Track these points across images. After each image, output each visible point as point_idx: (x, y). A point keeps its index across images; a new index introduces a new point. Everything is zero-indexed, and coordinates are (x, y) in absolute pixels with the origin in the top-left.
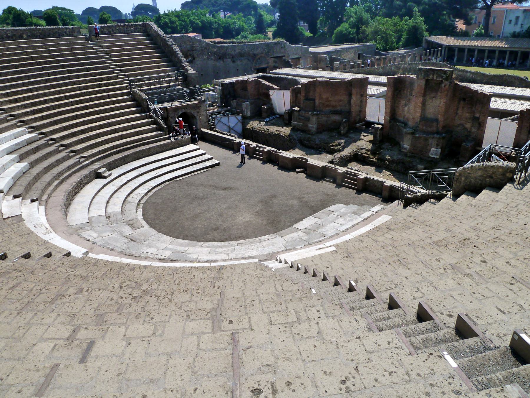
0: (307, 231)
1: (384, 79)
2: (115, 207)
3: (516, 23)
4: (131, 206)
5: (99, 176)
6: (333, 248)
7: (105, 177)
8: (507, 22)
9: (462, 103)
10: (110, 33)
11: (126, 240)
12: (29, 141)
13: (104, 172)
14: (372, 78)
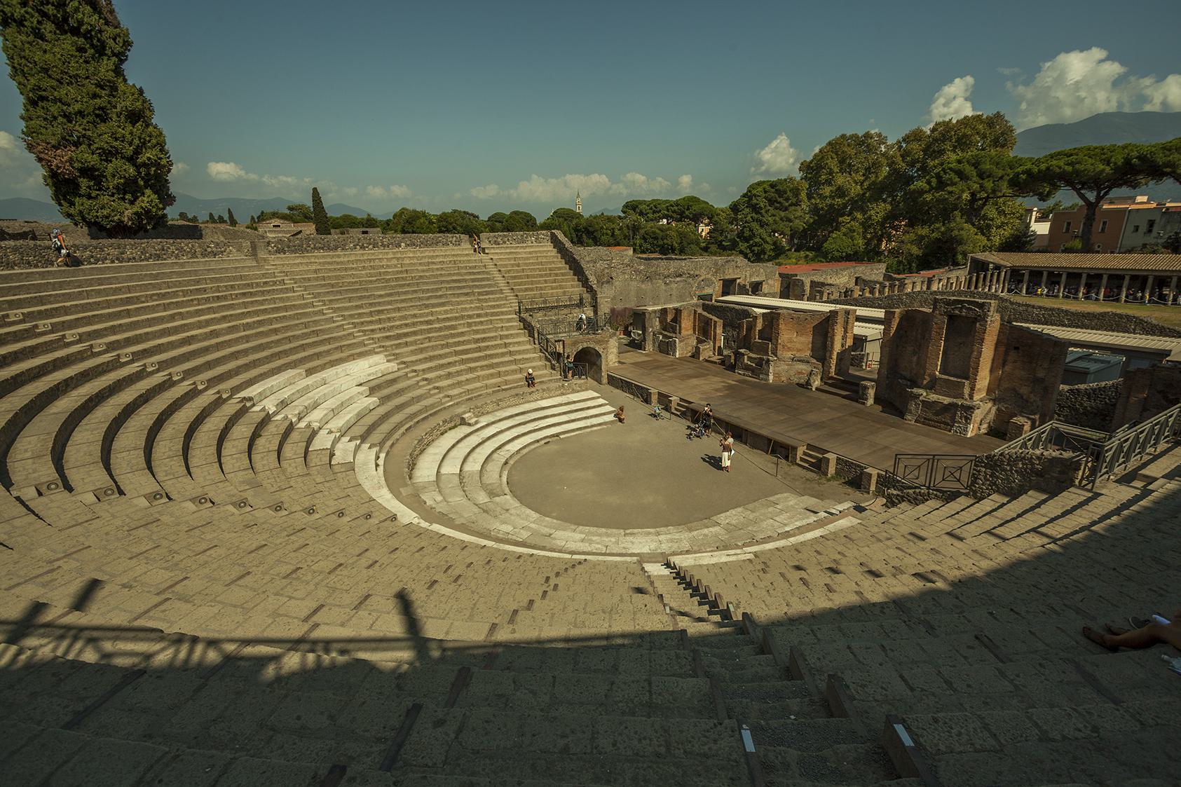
0: (730, 529)
1: (880, 313)
2: (474, 466)
3: (1150, 231)
4: (494, 468)
5: (463, 422)
6: (751, 556)
7: (469, 425)
8: (1131, 228)
9: (1013, 354)
11: (476, 510)
14: (862, 311)
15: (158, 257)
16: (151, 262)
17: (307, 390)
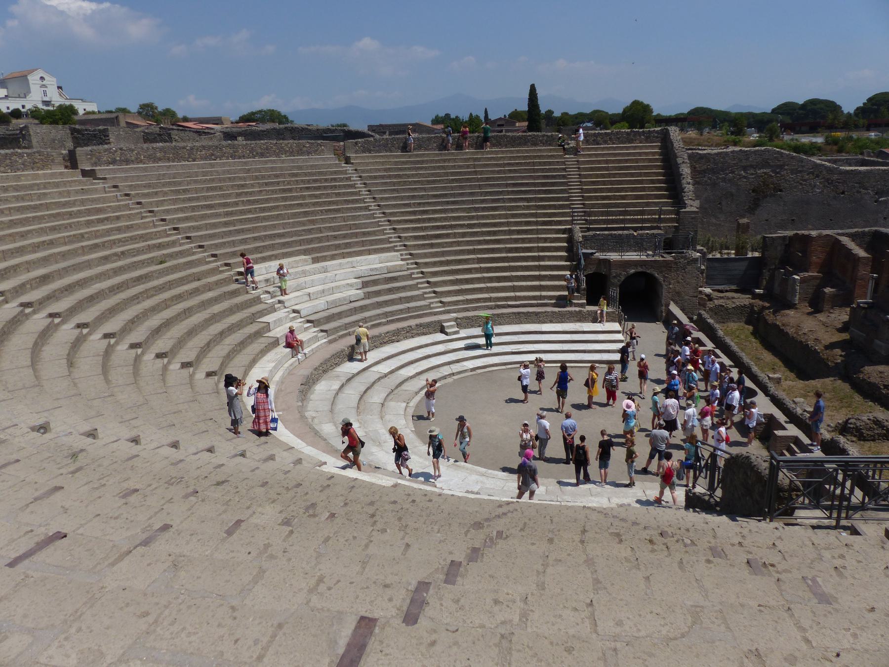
5: (442, 330)
7: (446, 334)
10: (605, 142)
12: (392, 270)
13: (452, 326)
15: (262, 155)
16: (257, 159)
17: (304, 273)
